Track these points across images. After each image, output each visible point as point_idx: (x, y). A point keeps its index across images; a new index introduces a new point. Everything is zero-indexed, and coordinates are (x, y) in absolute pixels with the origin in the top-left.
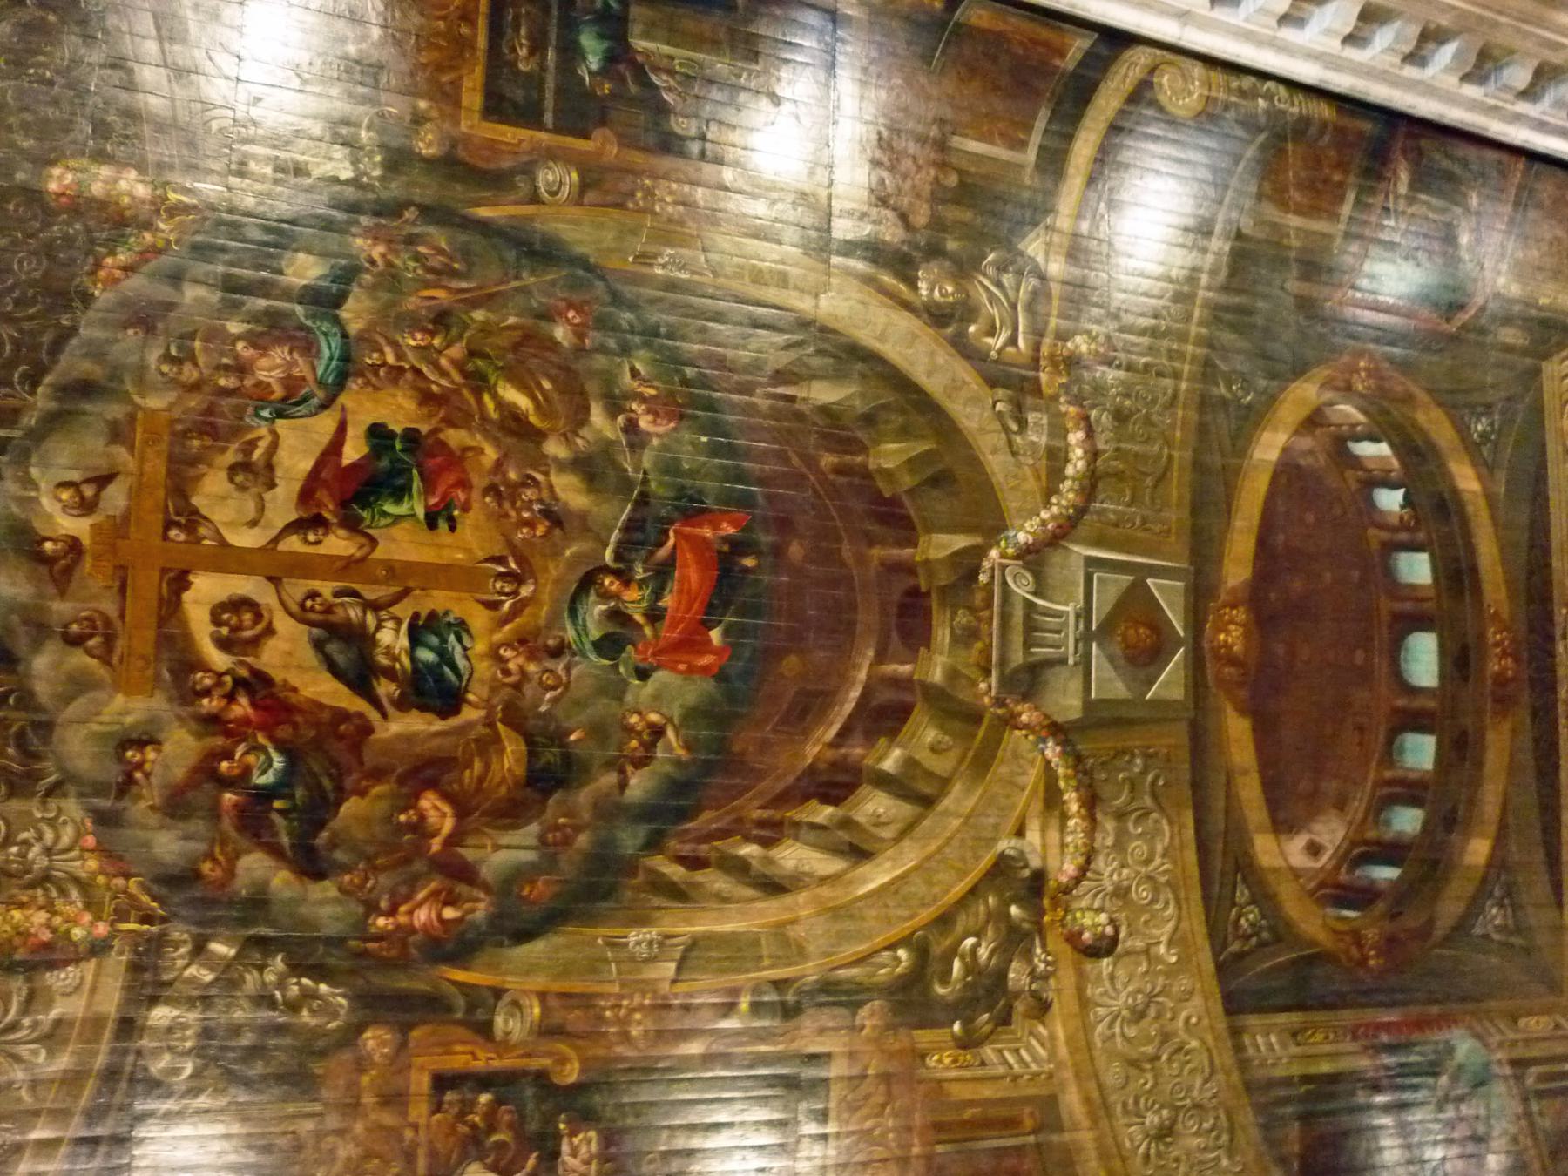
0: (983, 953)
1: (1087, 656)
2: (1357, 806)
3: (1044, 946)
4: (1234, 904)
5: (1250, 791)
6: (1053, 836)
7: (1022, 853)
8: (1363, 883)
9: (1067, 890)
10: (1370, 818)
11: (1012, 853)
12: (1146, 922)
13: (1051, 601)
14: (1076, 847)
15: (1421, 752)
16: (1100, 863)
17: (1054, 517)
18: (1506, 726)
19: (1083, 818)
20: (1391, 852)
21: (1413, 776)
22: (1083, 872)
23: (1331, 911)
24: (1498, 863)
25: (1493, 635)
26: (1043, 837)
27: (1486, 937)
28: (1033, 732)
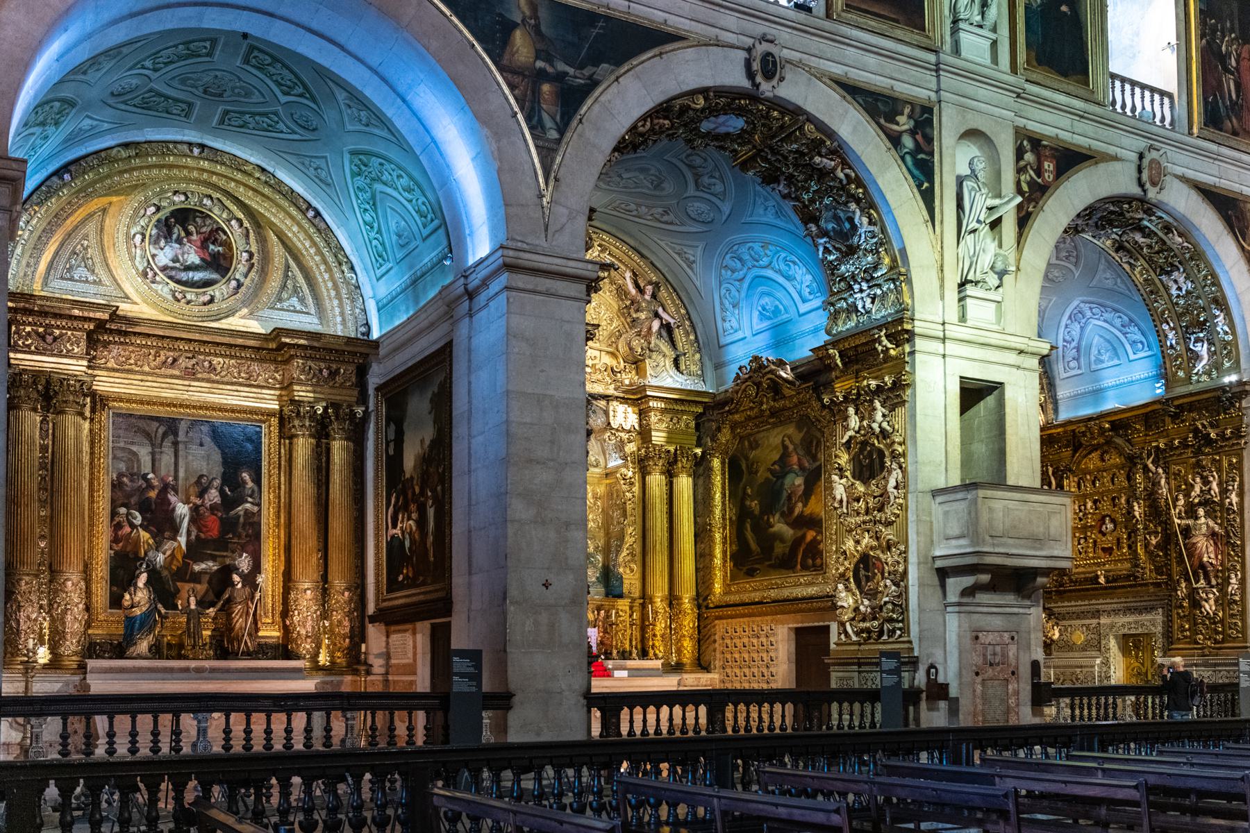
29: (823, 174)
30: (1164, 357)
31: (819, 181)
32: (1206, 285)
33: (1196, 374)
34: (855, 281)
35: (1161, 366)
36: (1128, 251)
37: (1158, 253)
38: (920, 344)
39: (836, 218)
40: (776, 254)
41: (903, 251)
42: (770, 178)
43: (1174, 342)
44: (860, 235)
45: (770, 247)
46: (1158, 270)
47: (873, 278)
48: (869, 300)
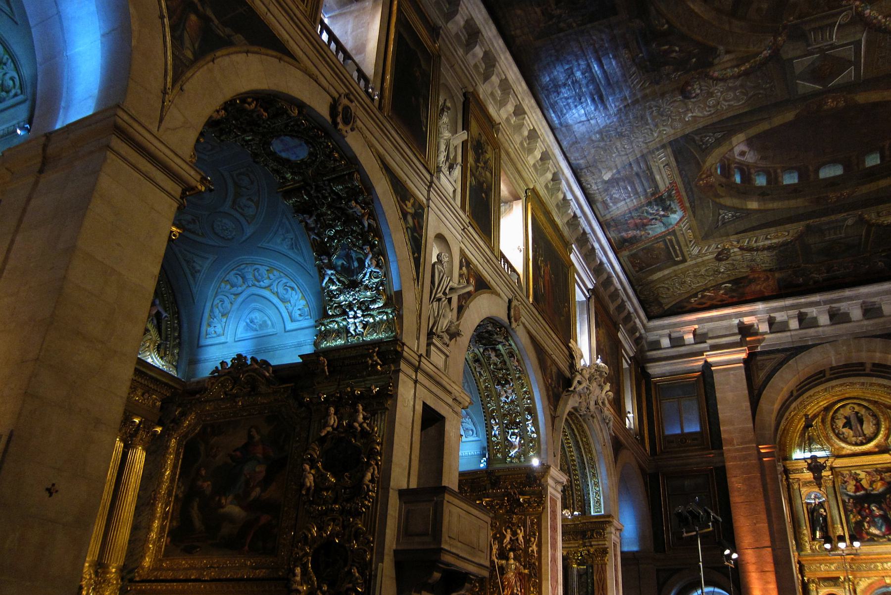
0: (674, 55)
1: (813, 54)
2: (762, 164)
3: (680, 75)
4: (714, 133)
5: (764, 126)
6: (729, 64)
7: (719, 56)
8: (732, 172)
9: (707, 75)
10: (759, 169)
11: (718, 53)
12: (699, 106)
13: (837, 32)
14: (725, 74)
15: (790, 179)
16: (721, 84)
17: (879, 21)
18: (807, 204)
19: (739, 73)
20: (747, 178)
21: (780, 179)
22: (717, 80)
23: (718, 164)
24: (750, 212)
25: (845, 193)
26: (727, 62)
27: (720, 214)
28: (774, 44)
29: (349, 219)
30: (488, 442)
31: (344, 224)
32: (523, 399)
33: (510, 457)
34: (352, 309)
35: (484, 448)
36: (481, 364)
37: (501, 369)
38: (403, 366)
39: (348, 257)
40: (278, 278)
41: (399, 294)
42: (303, 209)
43: (497, 432)
44: (365, 274)
45: (275, 272)
46: (496, 382)
47: (368, 309)
48: (361, 326)
